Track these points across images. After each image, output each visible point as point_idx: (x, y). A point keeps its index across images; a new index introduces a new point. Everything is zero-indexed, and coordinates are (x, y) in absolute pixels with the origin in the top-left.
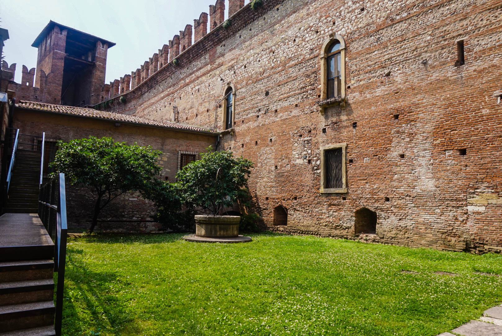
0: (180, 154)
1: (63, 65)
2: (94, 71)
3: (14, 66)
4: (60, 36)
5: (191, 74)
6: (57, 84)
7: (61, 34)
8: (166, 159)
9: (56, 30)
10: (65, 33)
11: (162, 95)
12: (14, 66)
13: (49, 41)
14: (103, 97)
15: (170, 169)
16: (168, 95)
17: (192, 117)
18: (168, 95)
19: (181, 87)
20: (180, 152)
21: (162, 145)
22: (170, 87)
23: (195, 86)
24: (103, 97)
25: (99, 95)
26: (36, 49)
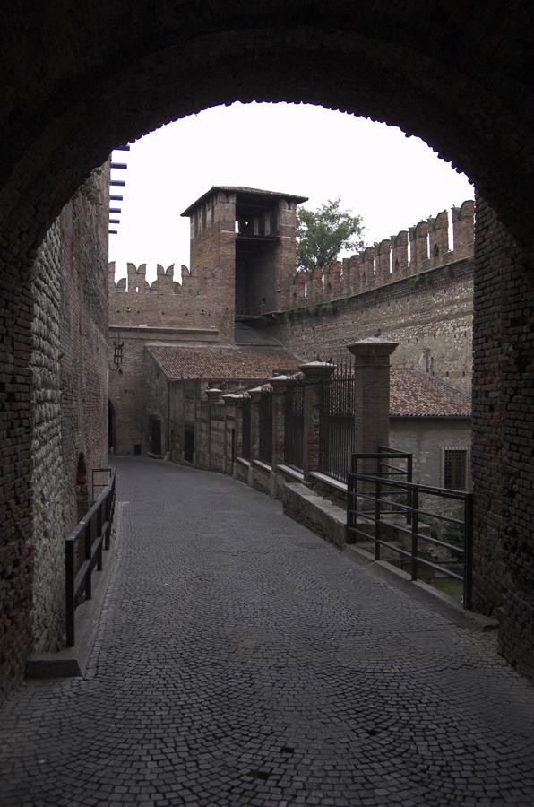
0: (443, 452)
1: (234, 253)
2: (278, 251)
3: (171, 268)
4: (227, 206)
5: (451, 303)
6: (229, 285)
7: (228, 202)
8: (424, 461)
9: (221, 198)
10: (233, 200)
11: (403, 321)
12: (171, 268)
13: (209, 214)
14: (295, 294)
15: (430, 474)
16: (413, 324)
17: (457, 375)
18: (413, 324)
19: (434, 318)
20: (443, 449)
21: (419, 441)
22: (415, 312)
23: (459, 326)
24: (295, 294)
25: (288, 290)
26: (188, 219)
